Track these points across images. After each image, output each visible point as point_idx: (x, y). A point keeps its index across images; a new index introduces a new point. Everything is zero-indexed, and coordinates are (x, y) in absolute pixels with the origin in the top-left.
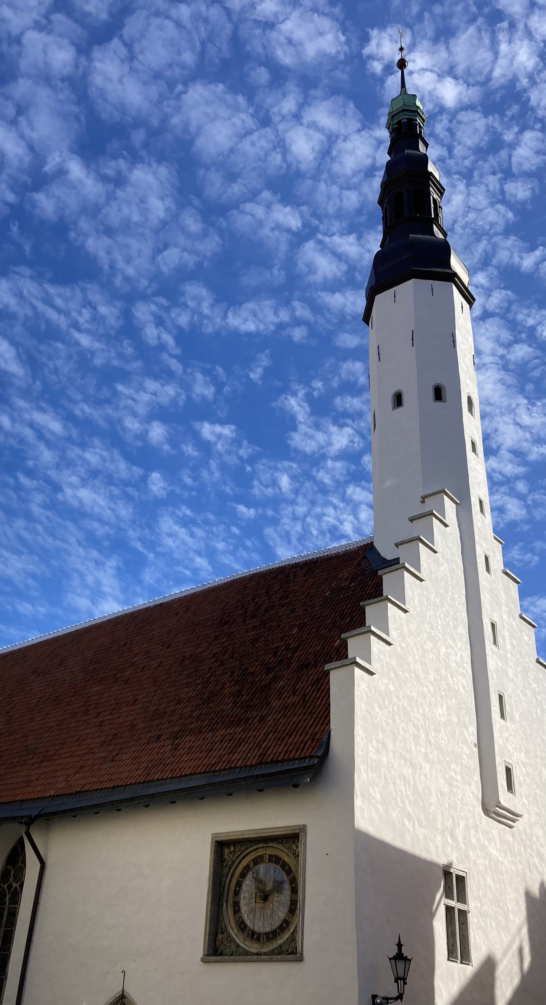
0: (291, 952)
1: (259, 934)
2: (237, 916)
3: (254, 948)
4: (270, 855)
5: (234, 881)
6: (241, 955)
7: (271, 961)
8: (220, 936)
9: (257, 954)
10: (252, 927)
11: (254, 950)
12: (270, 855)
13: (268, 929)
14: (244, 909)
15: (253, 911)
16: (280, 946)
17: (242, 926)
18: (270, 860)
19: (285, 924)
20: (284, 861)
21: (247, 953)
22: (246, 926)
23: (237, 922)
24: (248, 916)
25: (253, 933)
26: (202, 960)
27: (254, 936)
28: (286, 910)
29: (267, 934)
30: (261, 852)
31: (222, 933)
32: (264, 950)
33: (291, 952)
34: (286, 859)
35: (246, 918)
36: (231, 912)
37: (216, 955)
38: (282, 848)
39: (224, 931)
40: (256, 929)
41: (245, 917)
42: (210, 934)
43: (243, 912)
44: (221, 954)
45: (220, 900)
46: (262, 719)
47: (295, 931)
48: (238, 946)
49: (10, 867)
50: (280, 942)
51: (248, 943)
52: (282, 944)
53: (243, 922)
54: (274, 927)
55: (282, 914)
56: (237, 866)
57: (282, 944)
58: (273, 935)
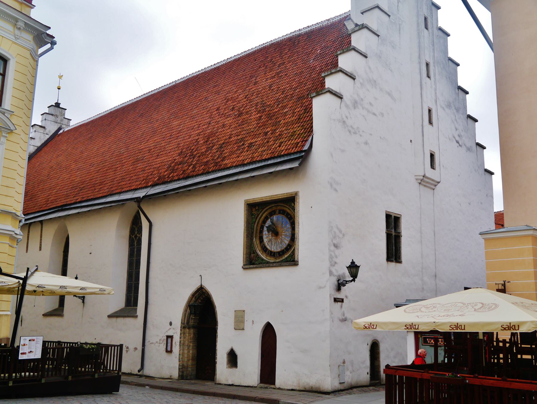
0: (292, 261)
1: (275, 252)
2: (262, 244)
3: (272, 260)
5: (259, 225)
8: (252, 255)
9: (273, 263)
11: (272, 261)
13: (279, 250)
14: (265, 240)
15: (270, 241)
16: (286, 258)
17: (264, 249)
18: (279, 213)
20: (287, 213)
21: (268, 262)
22: (267, 249)
23: (262, 247)
25: (271, 252)
26: (243, 268)
27: (272, 254)
28: (289, 239)
29: (279, 252)
30: (274, 208)
31: (254, 253)
32: (277, 261)
33: (292, 261)
34: (289, 211)
36: (258, 242)
39: (255, 252)
40: (273, 250)
42: (246, 254)
43: (265, 242)
44: (254, 264)
45: (252, 236)
46: (274, 132)
47: (294, 249)
49: (134, 226)
50: (286, 256)
51: (268, 258)
52: (287, 257)
53: (265, 247)
54: (283, 249)
55: (287, 241)
56: (261, 217)
57: (287, 257)
58: (281, 253)
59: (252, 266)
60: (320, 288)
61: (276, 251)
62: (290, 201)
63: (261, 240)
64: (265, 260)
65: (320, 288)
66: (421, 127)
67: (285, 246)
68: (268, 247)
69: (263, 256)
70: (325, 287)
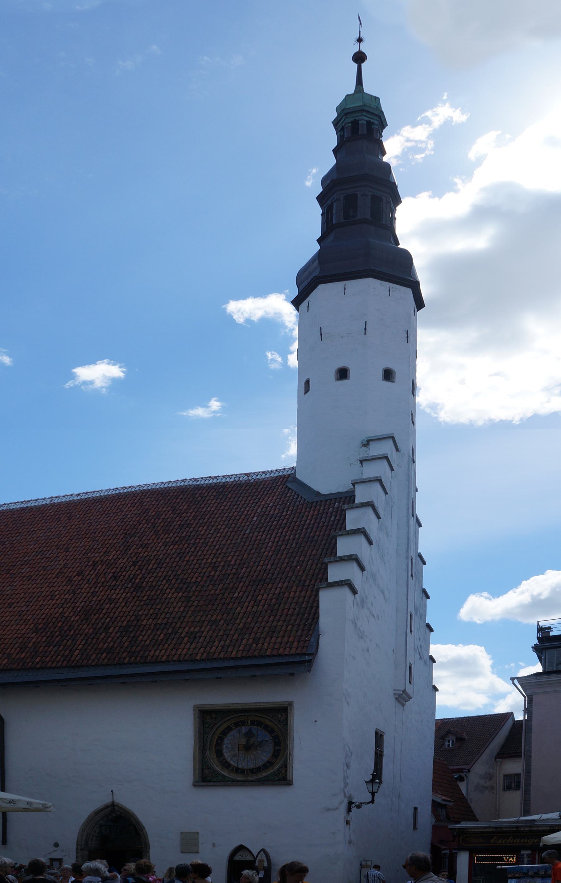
4: (251, 721)
6: (224, 782)
7: (253, 785)
10: (236, 765)
12: (251, 721)
14: (227, 755)
17: (226, 765)
19: (268, 765)
22: (230, 765)
24: (231, 759)
34: (269, 723)
35: (230, 759)
37: (203, 782)
38: (265, 716)
40: (240, 766)
41: (229, 760)
43: (226, 756)
48: (224, 777)
50: (264, 774)
53: (226, 762)
59: (203, 784)
60: (328, 810)
61: (245, 767)
62: (283, 712)
63: (219, 754)
64: (228, 777)
65: (328, 810)
66: (405, 635)
67: (261, 763)
68: (232, 763)
69: (226, 773)
70: (337, 809)
